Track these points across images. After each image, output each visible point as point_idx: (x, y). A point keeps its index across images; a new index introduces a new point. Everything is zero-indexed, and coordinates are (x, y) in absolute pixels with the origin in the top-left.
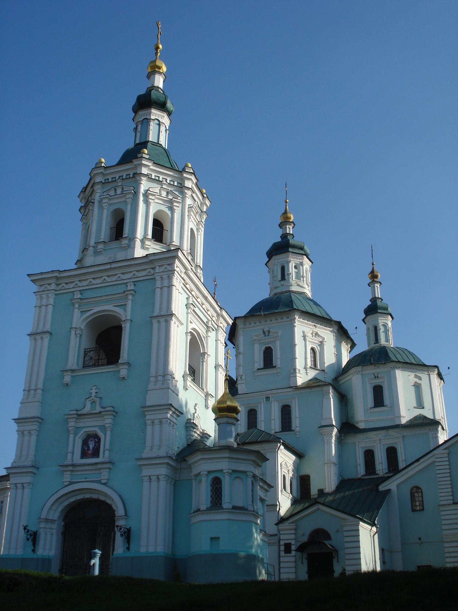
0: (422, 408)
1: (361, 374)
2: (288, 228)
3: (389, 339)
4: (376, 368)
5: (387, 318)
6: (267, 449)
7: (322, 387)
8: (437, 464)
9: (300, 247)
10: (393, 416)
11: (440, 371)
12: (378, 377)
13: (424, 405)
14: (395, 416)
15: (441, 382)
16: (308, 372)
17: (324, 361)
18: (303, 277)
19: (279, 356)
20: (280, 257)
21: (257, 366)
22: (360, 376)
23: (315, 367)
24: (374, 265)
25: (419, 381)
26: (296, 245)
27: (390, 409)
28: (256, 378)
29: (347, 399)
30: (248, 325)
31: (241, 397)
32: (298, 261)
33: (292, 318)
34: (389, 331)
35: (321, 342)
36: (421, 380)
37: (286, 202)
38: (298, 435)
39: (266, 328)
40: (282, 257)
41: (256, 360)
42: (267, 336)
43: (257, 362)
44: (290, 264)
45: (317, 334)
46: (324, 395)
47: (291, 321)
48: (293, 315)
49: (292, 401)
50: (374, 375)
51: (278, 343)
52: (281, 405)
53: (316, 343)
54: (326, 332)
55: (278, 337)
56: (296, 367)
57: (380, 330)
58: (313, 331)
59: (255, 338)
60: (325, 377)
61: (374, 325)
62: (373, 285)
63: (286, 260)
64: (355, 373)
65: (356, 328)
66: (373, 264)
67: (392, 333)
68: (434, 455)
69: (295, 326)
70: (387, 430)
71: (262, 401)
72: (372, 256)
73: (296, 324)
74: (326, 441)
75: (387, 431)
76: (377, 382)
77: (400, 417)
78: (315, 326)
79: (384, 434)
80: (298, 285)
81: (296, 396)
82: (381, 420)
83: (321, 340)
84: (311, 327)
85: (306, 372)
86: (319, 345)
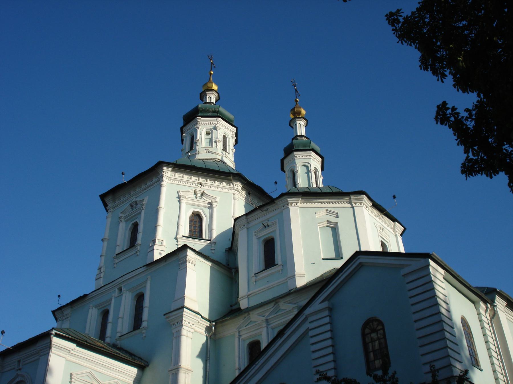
0: (340, 258)
1: (248, 228)
2: (208, 98)
3: (311, 182)
4: (265, 212)
5: (310, 156)
6: (41, 350)
8: (311, 333)
9: (213, 110)
10: (286, 278)
11: (375, 202)
12: (268, 226)
13: (342, 255)
14: (288, 276)
15: (394, 225)
18: (216, 142)
23: (199, 237)
24: (298, 101)
25: (333, 219)
28: (115, 267)
30: (117, 202)
31: (94, 295)
32: (212, 126)
33: (160, 175)
34: (311, 172)
35: (210, 204)
36: (337, 217)
37: (211, 74)
38: (144, 333)
40: (191, 126)
43: (119, 246)
50: (262, 225)
52: (135, 294)
54: (221, 190)
55: (143, 205)
57: (297, 173)
58: (195, 190)
59: (121, 215)
60: (212, 249)
65: (276, 183)
67: (321, 176)
68: (306, 319)
70: (277, 303)
71: (114, 294)
73: (163, 183)
74: (175, 335)
75: (275, 305)
76: (266, 233)
77: (294, 276)
78: (201, 184)
79: (272, 309)
80: (209, 152)
82: (270, 288)
83: (210, 201)
84: (194, 185)
85: (177, 243)
86: (209, 208)
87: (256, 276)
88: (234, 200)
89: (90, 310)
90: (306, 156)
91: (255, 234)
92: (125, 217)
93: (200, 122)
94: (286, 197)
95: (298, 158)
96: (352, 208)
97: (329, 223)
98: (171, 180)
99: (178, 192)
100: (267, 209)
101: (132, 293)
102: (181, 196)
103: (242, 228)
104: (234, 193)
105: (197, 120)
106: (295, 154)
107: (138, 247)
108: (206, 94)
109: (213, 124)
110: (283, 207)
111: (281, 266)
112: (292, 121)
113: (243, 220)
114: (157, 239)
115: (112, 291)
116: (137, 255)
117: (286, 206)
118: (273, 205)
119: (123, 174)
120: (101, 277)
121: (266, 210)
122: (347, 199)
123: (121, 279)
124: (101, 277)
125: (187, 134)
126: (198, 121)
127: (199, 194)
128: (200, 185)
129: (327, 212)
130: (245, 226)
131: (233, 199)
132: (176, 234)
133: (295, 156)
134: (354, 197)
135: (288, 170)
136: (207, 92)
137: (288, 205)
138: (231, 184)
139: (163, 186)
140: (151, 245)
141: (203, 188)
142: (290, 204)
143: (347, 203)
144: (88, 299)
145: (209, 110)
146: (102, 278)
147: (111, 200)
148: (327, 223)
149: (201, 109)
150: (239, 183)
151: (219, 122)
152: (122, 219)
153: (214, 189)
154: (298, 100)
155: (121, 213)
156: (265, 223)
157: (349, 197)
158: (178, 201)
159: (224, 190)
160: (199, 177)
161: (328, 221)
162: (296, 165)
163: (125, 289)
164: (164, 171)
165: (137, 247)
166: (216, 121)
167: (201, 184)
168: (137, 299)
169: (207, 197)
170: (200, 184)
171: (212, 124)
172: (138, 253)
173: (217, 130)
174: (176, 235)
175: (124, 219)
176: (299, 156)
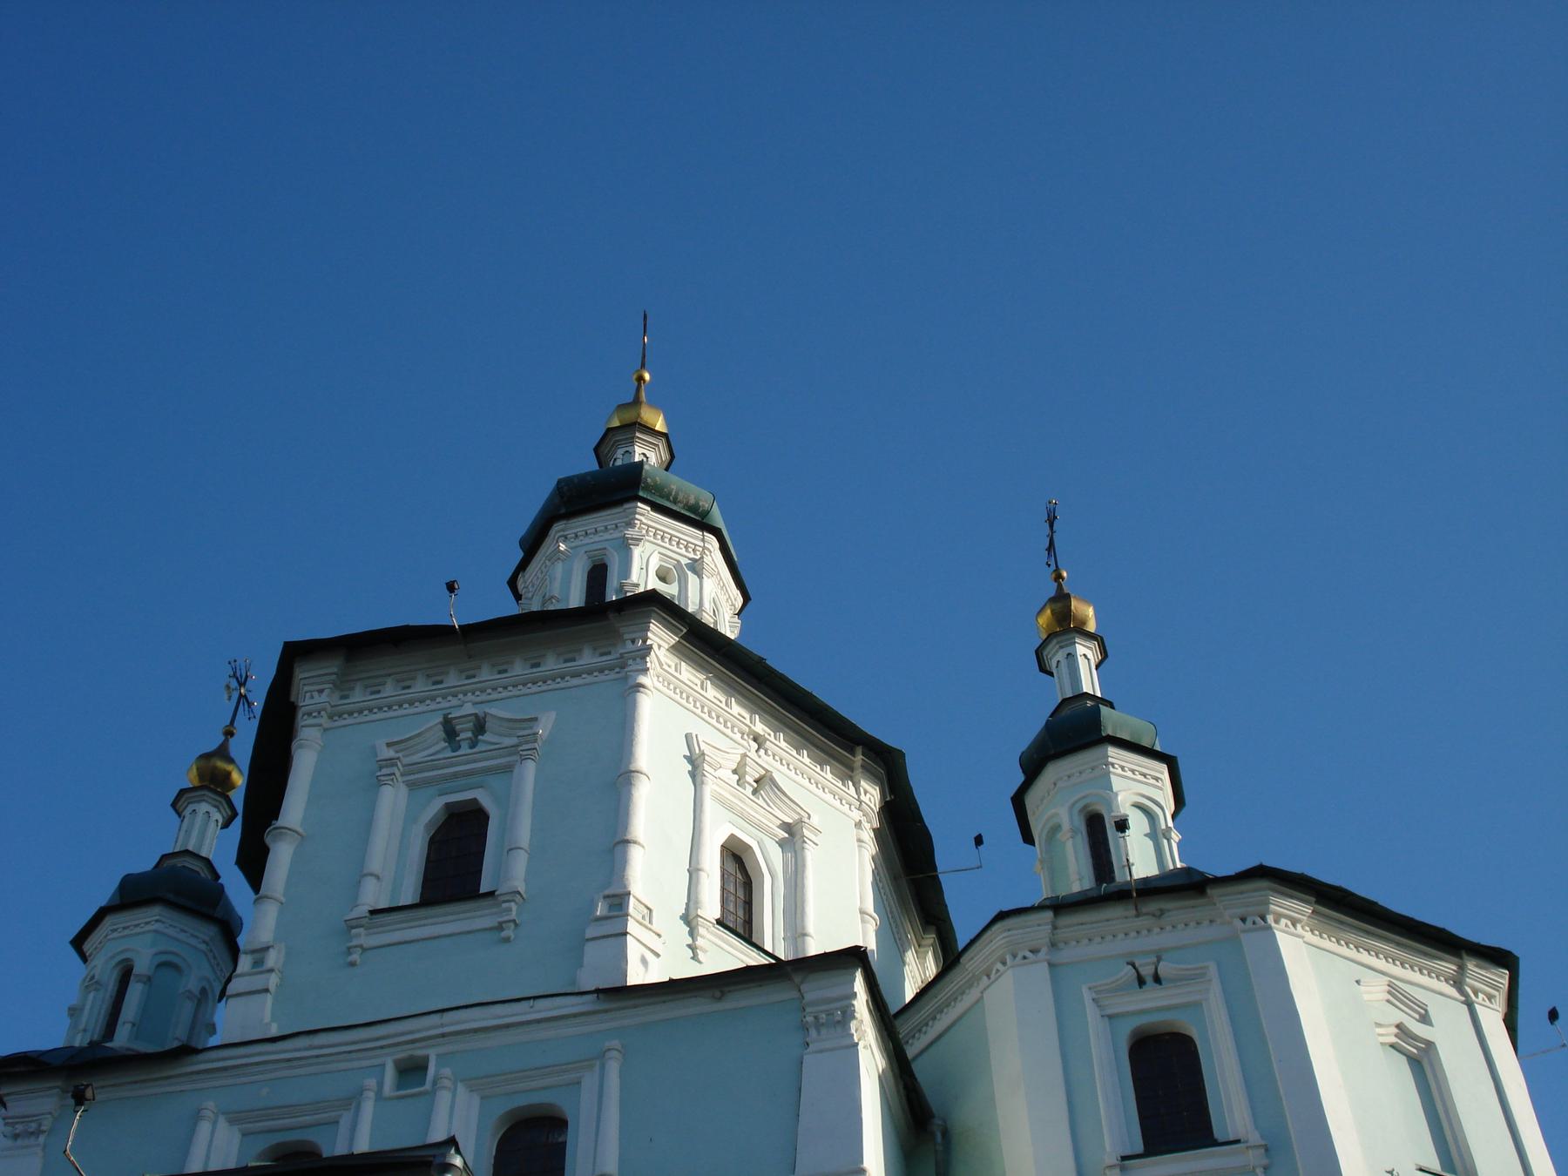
1: (1051, 965)
7: (797, 979)
9: (692, 501)
12: (1157, 979)
16: (700, 942)
17: (803, 928)
19: (524, 832)
20: (590, 528)
21: (374, 895)
22: (1039, 972)
26: (674, 487)
27: (1265, 1161)
28: (353, 964)
29: (946, 1133)
30: (358, 696)
37: (641, 379)
39: (470, 704)
40: (600, 525)
41: (375, 863)
42: (464, 745)
43: (378, 878)
44: (637, 552)
45: (764, 782)
46: (813, 1032)
47: (623, 666)
48: (633, 636)
49: (579, 1083)
50: (1130, 967)
51: (530, 769)
52: (503, 1106)
53: (759, 827)
55: (535, 741)
56: (625, 886)
58: (744, 756)
61: (1085, 807)
62: (1068, 650)
63: (617, 534)
64: (1008, 958)
66: (1058, 577)
69: (639, 686)
71: (371, 1082)
72: (1051, 547)
81: (616, 1043)
84: (738, 737)
85: (690, 941)
86: (782, 844)
87: (1123, 1169)
88: (859, 846)
89: (204, 1128)
90: (1145, 775)
91: (1094, 996)
92: (411, 769)
93: (642, 523)
94: (1264, 884)
95: (1119, 771)
96: (1465, 1007)
97: (1403, 1036)
98: (666, 684)
99: (688, 737)
100: (1162, 912)
101: (482, 1098)
102: (706, 758)
103: (1025, 958)
104: (860, 821)
105: (636, 513)
106: (1110, 753)
107: (513, 904)
108: (633, 438)
109: (687, 551)
110: (1238, 923)
111: (1263, 1151)
112: (1059, 639)
113: (1039, 925)
114: (634, 897)
115: (356, 1064)
116: (507, 940)
117: (1254, 923)
118: (1192, 902)
119: (451, 587)
120: (267, 990)
121: (1158, 913)
122: (1449, 967)
123: (435, 1019)
124: (267, 990)
125: (571, 548)
126: (637, 516)
127: (751, 776)
128: (756, 746)
129: (1389, 992)
130: (1042, 954)
131: (856, 844)
132: (686, 901)
133: (1110, 759)
134: (1477, 966)
135: (1076, 802)
136: (638, 434)
137: (1263, 918)
138: (850, 783)
139: (646, 694)
140: (598, 913)
141: (767, 761)
142: (1270, 919)
143: (1446, 981)
144: (189, 1069)
145: (677, 494)
146: (269, 998)
147: (334, 677)
148: (1396, 1036)
149: (649, 480)
150: (878, 789)
151: (711, 552)
152: (398, 774)
153: (799, 778)
154: (1065, 574)
155: (389, 745)
156: (1141, 966)
157: (1456, 960)
158: (689, 771)
159: (829, 797)
160: (752, 712)
161: (1398, 1026)
162: (1116, 794)
163: (447, 1071)
164: (649, 634)
165: (504, 905)
166: (702, 544)
167: (760, 740)
168: (499, 1136)
169: (778, 801)
170: (755, 740)
171: (684, 549)
172: (509, 932)
173: (700, 577)
174: (687, 909)
175: (402, 775)
176: (1123, 768)
